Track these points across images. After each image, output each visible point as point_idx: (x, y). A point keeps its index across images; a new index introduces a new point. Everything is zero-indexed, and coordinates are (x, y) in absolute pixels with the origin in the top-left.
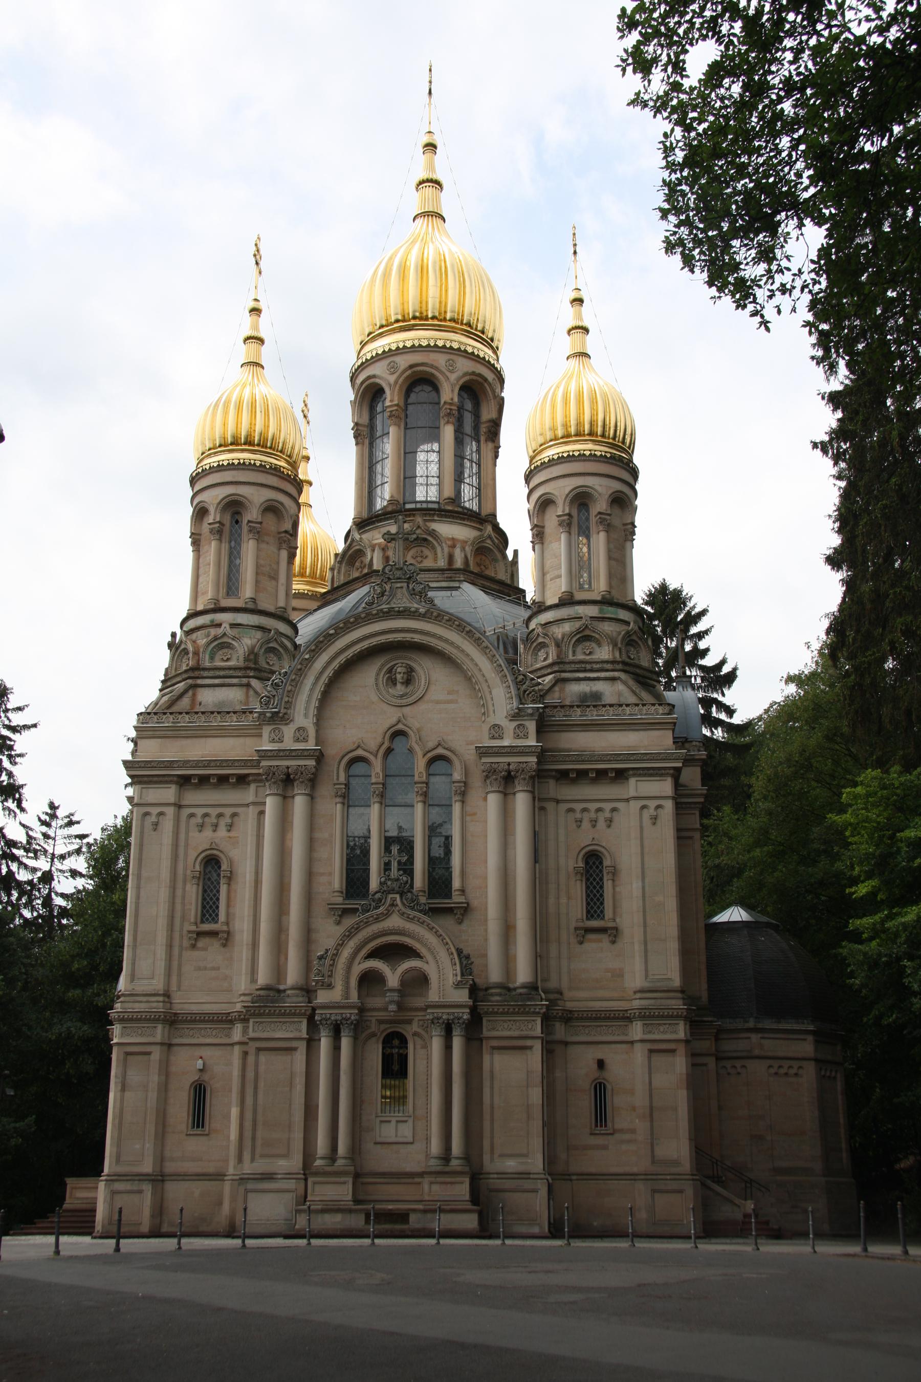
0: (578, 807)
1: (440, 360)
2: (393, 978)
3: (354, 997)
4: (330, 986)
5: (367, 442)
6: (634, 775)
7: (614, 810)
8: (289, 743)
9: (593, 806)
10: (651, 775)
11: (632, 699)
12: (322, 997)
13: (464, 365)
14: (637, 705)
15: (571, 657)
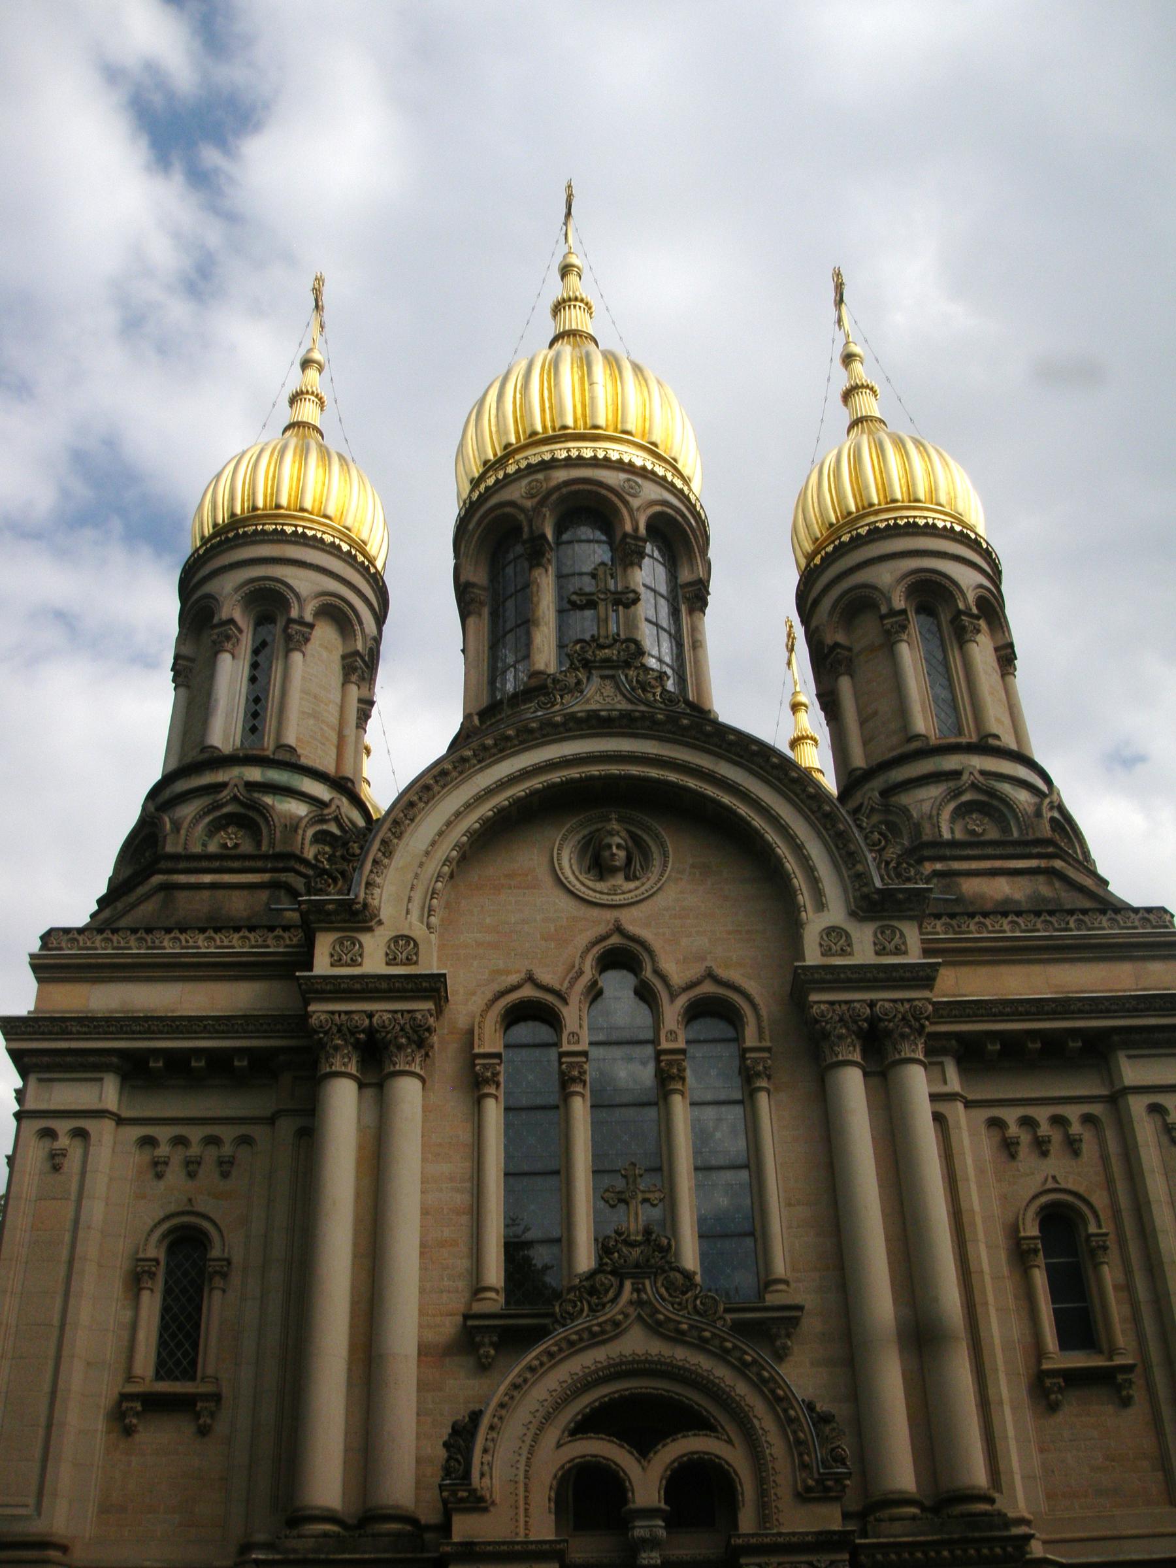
0: (1011, 1116)
1: (613, 478)
2: (646, 1484)
3: (543, 1528)
4: (478, 1504)
5: (486, 611)
6: (1127, 1045)
7: (1088, 1119)
8: (374, 960)
9: (1042, 1114)
10: (1156, 1044)
11: (1087, 904)
12: (464, 1528)
13: (651, 492)
14: (1103, 912)
15: (947, 835)
